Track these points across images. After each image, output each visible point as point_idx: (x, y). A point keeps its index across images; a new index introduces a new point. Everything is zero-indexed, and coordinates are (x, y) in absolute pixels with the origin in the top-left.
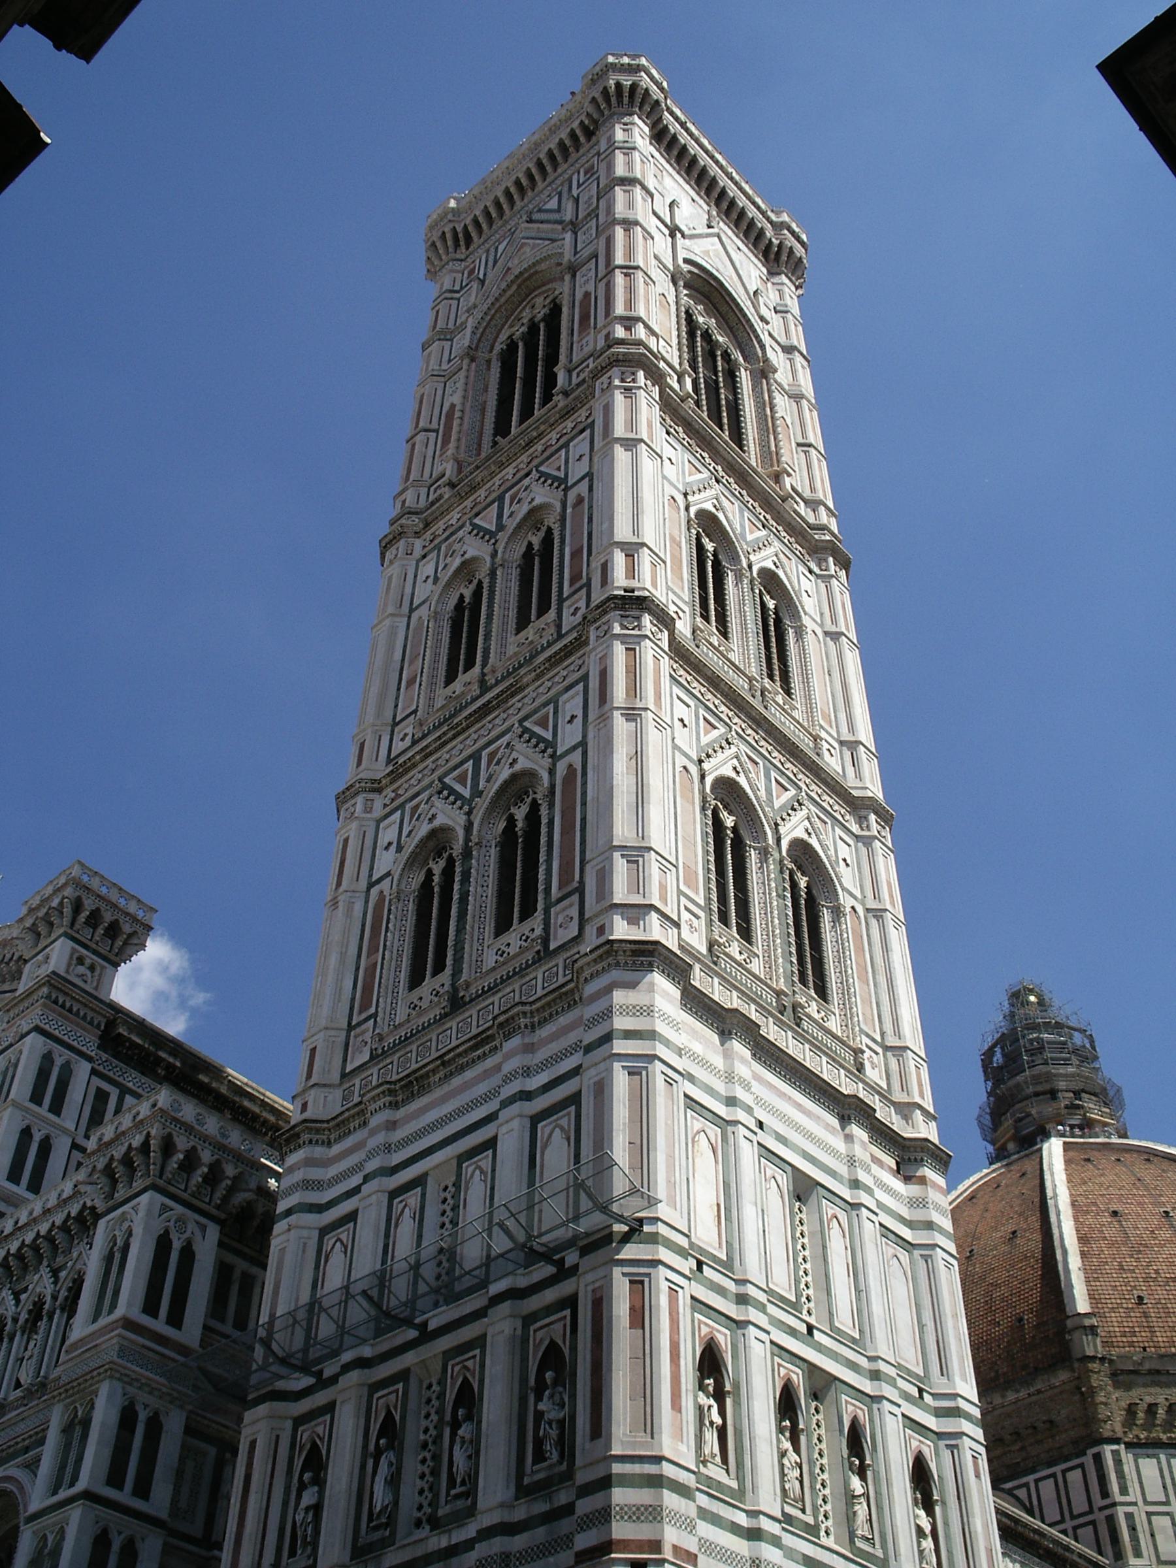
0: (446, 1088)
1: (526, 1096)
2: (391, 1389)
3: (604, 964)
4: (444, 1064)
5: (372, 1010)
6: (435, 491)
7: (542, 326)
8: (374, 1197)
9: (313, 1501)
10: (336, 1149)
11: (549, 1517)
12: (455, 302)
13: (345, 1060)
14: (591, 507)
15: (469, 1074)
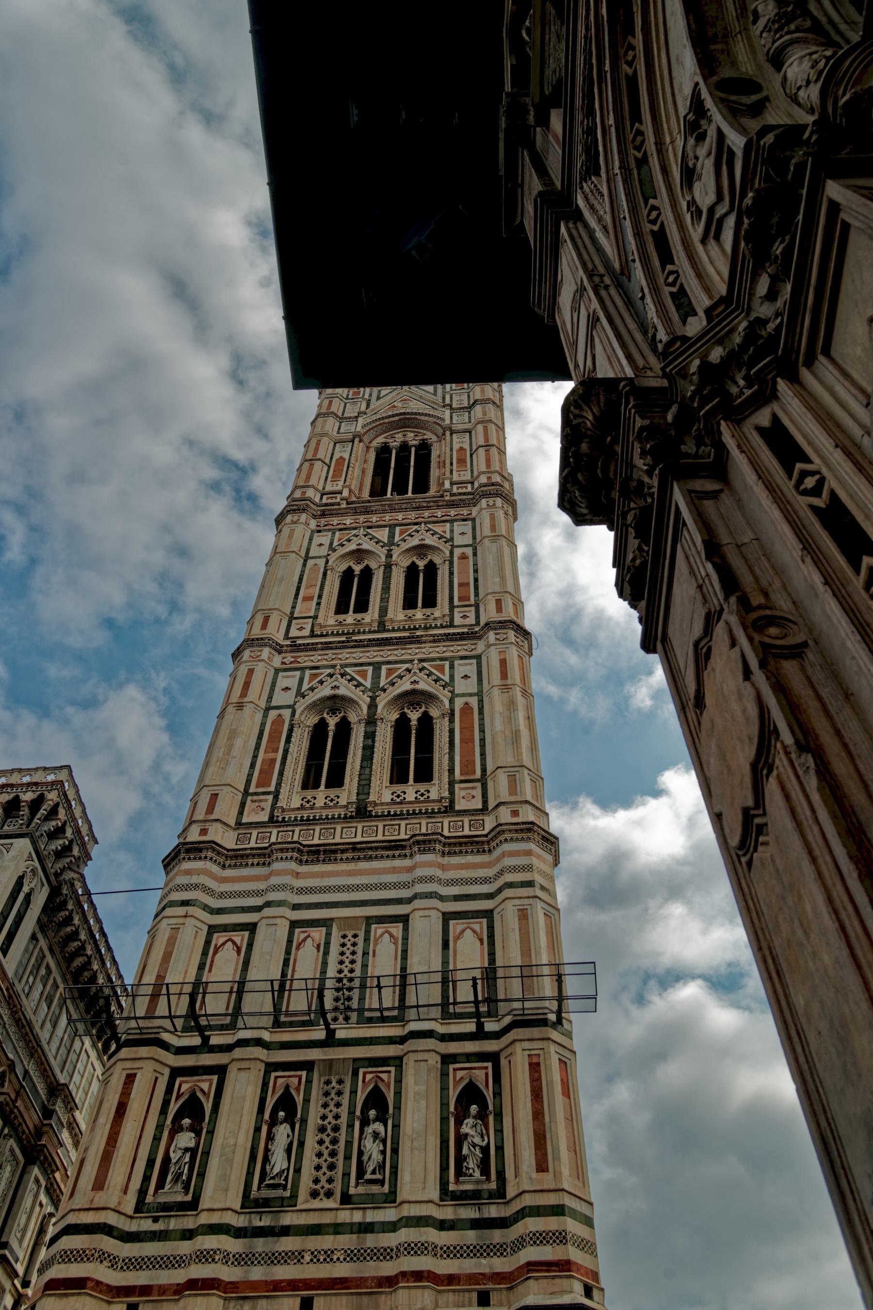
0: (351, 866)
1: (442, 898)
2: (292, 1073)
3: (525, 835)
4: (354, 849)
5: (272, 788)
6: (328, 498)
7: (413, 450)
8: (278, 921)
9: (192, 1144)
10: (229, 873)
11: (477, 1224)
12: (342, 405)
13: (241, 813)
14: (475, 565)
15: (376, 864)
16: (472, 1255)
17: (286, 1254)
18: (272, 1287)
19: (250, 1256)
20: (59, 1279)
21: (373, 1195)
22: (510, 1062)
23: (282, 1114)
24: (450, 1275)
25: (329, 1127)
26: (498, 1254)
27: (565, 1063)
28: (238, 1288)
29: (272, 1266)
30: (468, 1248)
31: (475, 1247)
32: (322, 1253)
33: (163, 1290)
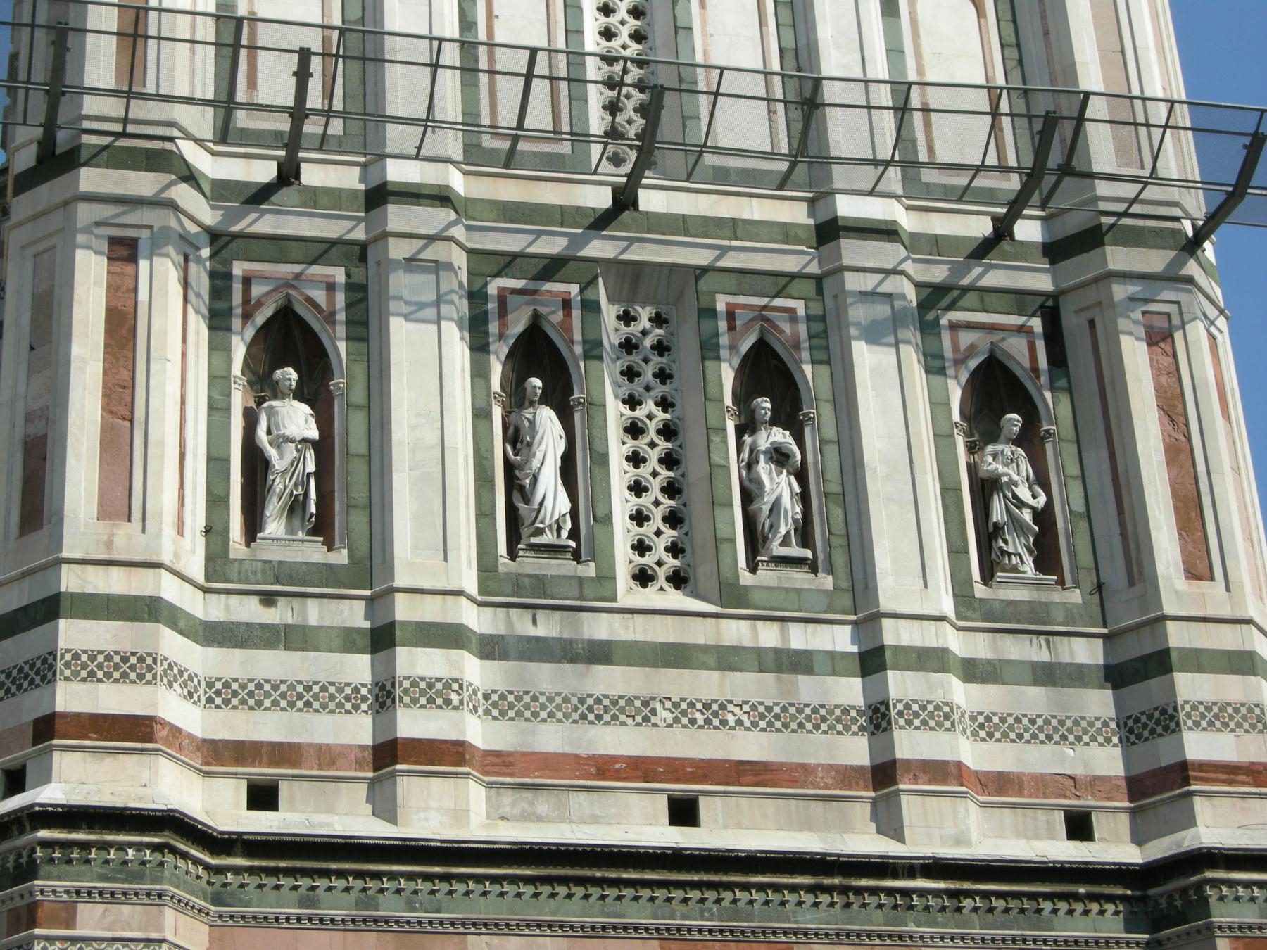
9: (314, 434)
16: (1042, 737)
17: (614, 702)
18: (593, 770)
19: (527, 699)
20: (78, 716)
21: (799, 591)
22: (1092, 323)
23: (537, 382)
24: (999, 773)
25: (652, 426)
26: (1101, 739)
27: (1214, 338)
28: (511, 764)
29: (584, 726)
30: (1033, 722)
31: (1047, 722)
32: (699, 706)
33: (327, 756)
